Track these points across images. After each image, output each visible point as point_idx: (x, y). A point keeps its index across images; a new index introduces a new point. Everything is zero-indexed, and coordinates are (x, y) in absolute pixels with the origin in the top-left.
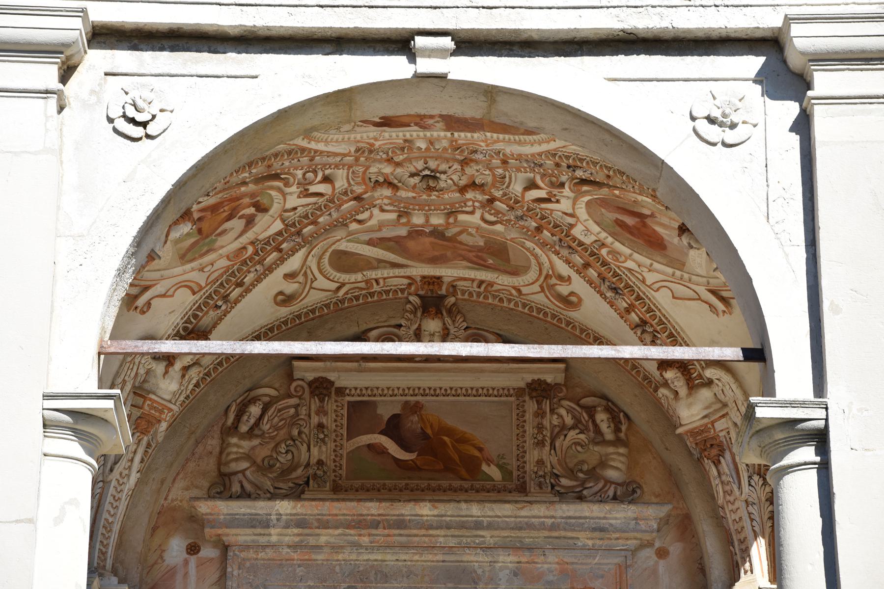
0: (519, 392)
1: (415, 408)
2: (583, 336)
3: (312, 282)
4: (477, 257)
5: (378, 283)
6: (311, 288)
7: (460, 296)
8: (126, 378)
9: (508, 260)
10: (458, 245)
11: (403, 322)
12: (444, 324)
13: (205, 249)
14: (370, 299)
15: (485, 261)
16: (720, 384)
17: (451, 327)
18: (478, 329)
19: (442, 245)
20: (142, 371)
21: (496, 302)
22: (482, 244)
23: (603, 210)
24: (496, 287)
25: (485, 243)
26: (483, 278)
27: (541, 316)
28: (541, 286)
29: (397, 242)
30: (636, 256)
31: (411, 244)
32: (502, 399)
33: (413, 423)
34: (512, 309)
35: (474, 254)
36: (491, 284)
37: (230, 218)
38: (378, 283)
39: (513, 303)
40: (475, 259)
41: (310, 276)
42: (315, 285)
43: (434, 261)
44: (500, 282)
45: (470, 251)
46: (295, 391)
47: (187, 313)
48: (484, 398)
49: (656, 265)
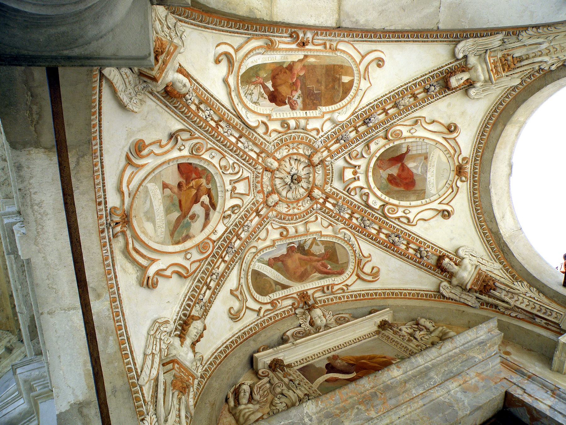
0: (377, 333)
1: (335, 357)
5: (279, 303)
8: (154, 351)
9: (337, 261)
10: (312, 257)
15: (326, 267)
19: (304, 260)
20: (164, 346)
22: (323, 251)
23: (381, 171)
24: (336, 288)
26: (328, 283)
27: (362, 298)
28: (358, 275)
29: (282, 261)
30: (402, 203)
32: (372, 338)
33: (339, 363)
34: (346, 301)
35: (320, 263)
36: (333, 285)
37: (196, 200)
38: (279, 303)
40: (321, 268)
43: (302, 277)
44: (337, 283)
45: (318, 261)
46: (262, 373)
48: (364, 341)
49: (413, 203)
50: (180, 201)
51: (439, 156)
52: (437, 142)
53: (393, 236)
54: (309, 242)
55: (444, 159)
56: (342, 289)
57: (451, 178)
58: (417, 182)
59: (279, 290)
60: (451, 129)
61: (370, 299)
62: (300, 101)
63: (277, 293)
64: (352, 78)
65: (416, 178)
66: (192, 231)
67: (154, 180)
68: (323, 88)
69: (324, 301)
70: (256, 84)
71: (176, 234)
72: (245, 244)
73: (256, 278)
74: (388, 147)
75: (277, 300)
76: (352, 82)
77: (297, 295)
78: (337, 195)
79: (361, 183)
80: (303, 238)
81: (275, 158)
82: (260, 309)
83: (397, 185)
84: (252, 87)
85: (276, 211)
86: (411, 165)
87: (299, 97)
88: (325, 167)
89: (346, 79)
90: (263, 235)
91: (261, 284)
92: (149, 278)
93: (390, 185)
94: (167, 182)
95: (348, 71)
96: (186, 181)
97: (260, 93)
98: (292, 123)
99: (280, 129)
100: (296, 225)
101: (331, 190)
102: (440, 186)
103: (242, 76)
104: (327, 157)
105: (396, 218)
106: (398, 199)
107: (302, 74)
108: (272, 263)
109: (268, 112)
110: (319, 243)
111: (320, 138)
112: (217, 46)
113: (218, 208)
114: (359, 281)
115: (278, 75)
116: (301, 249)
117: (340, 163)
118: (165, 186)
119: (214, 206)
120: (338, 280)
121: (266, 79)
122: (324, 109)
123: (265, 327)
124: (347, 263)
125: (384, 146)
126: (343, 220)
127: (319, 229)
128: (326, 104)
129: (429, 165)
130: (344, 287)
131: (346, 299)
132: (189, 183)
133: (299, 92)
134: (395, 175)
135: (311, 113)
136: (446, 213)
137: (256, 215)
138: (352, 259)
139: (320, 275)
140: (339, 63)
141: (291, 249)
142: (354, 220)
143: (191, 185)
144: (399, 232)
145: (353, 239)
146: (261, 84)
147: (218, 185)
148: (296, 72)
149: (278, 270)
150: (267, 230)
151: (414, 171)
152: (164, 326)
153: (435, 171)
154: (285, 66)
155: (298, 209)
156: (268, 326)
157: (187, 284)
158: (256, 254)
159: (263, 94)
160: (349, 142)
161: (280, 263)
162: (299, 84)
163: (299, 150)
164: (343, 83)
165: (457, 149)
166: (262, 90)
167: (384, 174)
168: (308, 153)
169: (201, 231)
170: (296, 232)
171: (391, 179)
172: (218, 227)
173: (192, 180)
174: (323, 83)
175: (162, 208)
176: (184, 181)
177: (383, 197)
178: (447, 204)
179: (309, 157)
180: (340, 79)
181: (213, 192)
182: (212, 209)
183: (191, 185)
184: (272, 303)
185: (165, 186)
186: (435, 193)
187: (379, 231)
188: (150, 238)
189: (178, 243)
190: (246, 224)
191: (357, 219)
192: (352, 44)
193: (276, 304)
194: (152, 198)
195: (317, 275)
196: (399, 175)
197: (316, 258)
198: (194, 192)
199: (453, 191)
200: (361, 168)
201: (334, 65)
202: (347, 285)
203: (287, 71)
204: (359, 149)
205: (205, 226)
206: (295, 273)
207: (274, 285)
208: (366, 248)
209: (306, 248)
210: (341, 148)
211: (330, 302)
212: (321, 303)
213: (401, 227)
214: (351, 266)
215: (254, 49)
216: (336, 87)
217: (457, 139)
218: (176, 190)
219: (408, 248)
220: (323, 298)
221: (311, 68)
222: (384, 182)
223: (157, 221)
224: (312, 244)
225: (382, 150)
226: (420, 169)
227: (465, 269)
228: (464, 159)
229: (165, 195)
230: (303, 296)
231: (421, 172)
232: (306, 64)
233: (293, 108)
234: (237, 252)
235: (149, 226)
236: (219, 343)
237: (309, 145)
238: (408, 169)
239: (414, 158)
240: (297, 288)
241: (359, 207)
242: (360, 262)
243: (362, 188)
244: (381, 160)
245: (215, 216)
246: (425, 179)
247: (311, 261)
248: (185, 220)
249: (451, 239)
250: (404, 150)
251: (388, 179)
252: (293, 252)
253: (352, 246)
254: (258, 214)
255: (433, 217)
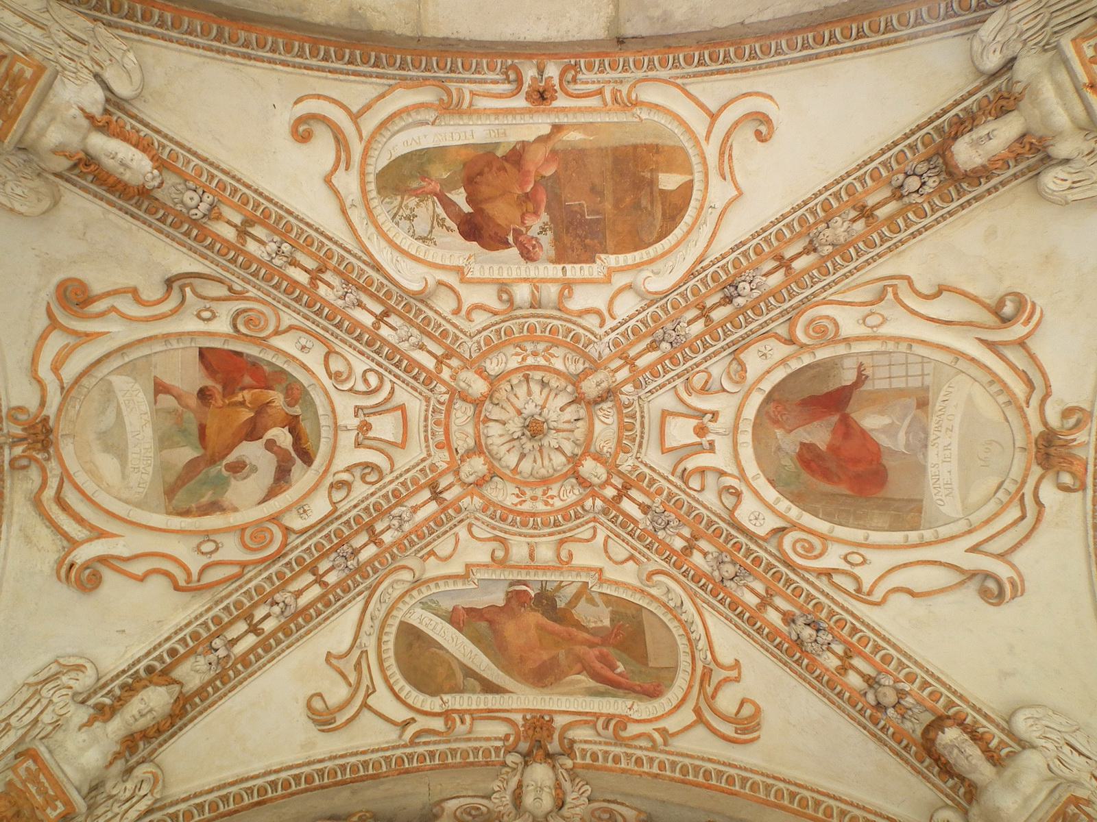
2: (772, 798)
3: (367, 695)
4: (603, 658)
5: (463, 722)
6: (365, 705)
7: (579, 761)
8: (13, 721)
9: (643, 659)
11: (496, 785)
12: (557, 780)
13: (205, 499)
14: (450, 761)
15: (613, 668)
16: (1050, 745)
17: (567, 785)
18: (609, 801)
19: (552, 633)
20: (47, 718)
21: (632, 766)
22: (607, 622)
23: (779, 433)
24: (633, 730)
25: (612, 620)
26: (612, 711)
27: (701, 779)
28: (697, 711)
29: (491, 622)
31: (510, 629)
34: (656, 776)
36: (623, 721)
37: (252, 432)
38: (463, 722)
39: (656, 764)
41: (366, 681)
42: (370, 701)
44: (636, 717)
45: (592, 645)
47: (160, 645)
49: (877, 537)
50: (202, 429)
51: (970, 399)
52: (959, 355)
53: (801, 621)
54: (570, 591)
55: (988, 407)
56: (650, 737)
57: (1016, 472)
58: (892, 476)
59: (474, 692)
60: (1008, 311)
61: (723, 791)
62: (546, 240)
63: (466, 696)
64: (686, 178)
65: (888, 462)
66: (230, 497)
67: (129, 369)
68: (608, 206)
69: (594, 756)
70: (421, 195)
71: (181, 495)
72: (388, 560)
73: (410, 646)
74: (795, 365)
75: (461, 713)
76: (688, 187)
77: (524, 718)
78: (652, 482)
79: (719, 459)
80: (554, 577)
81: (481, 372)
82: (406, 724)
83: (827, 475)
84: (413, 202)
85: (482, 497)
86: (871, 421)
87: (543, 230)
88: (620, 407)
89: (669, 181)
90: (444, 546)
91: (419, 660)
92: (72, 566)
93: (805, 476)
94: (167, 380)
95: (673, 158)
96: (224, 388)
97: (435, 216)
98: (522, 293)
99: (496, 305)
100: (537, 540)
101: (635, 468)
102: (975, 496)
103: (381, 176)
104: (625, 382)
105: (821, 573)
106: (828, 517)
107: (549, 172)
108: (463, 619)
109: (461, 262)
110: (598, 599)
111: (607, 333)
112: (296, 103)
113: (317, 462)
114: (700, 731)
115: (481, 174)
116: (545, 601)
117: (665, 400)
118: (160, 388)
119: (307, 458)
120: (643, 709)
121: (450, 184)
122: (612, 260)
123: (407, 772)
124: (673, 670)
125: (784, 362)
126: (664, 549)
127: (603, 565)
128: (620, 249)
129: (933, 425)
130: (656, 736)
131: (655, 770)
132: (233, 393)
133: (545, 217)
134: (823, 447)
135: (574, 271)
136: (991, 585)
137: (431, 499)
138: (684, 661)
139: (592, 683)
140: (650, 140)
141: (516, 598)
142: (697, 558)
143: (239, 398)
144: (823, 615)
145: (688, 605)
146: (436, 195)
147: (321, 411)
148: (532, 168)
149: (477, 640)
150: (456, 535)
151: (883, 440)
152: (73, 674)
153: (955, 448)
154: (500, 153)
155: (547, 503)
156: (418, 770)
157: (195, 607)
158: (417, 583)
159: (443, 220)
160: (681, 348)
161: (484, 624)
162: (543, 198)
163: (553, 360)
164: (662, 192)
165: (1037, 382)
166: (440, 210)
167: (789, 441)
168: (577, 367)
169: (259, 503)
170: (532, 557)
171: (809, 458)
172: (311, 502)
173: (243, 389)
174: (608, 194)
175: (149, 431)
176: (219, 387)
177: (784, 505)
178: (1001, 556)
179: (576, 380)
180: (652, 183)
181: (306, 426)
182: (299, 461)
183: (239, 398)
184: (446, 715)
185: (160, 388)
186: (954, 515)
187: (765, 602)
188: (108, 490)
189: (186, 513)
190: (395, 512)
191: (705, 554)
192: (677, 86)
193: (454, 721)
194: (123, 407)
195: (585, 680)
196: (833, 449)
197: (586, 635)
198: (246, 414)
199: (1023, 517)
200: (720, 419)
201: (635, 147)
202: (663, 732)
203: (507, 166)
204: (717, 368)
205: (271, 494)
206: (522, 660)
207: (459, 675)
208: (728, 641)
209: (561, 604)
210: (661, 361)
211: (610, 764)
212: (583, 758)
213: (833, 599)
214: (681, 681)
215: (406, 110)
216: (645, 202)
217: (1032, 344)
218: (193, 402)
219: (844, 669)
220: (596, 748)
221: (575, 158)
222: (790, 464)
223: (131, 456)
224: (577, 597)
225: (780, 375)
226: (902, 436)
227: (1012, 785)
228: (1067, 413)
229: (159, 406)
230: (539, 725)
231: (907, 445)
232: (559, 146)
233: (528, 255)
234: (359, 569)
235: (108, 465)
236: (257, 767)
237: (576, 346)
238: (863, 432)
239: (882, 400)
240: (525, 699)
241: (711, 523)
242: (707, 675)
243: (722, 473)
244: (779, 402)
245: (303, 478)
246: (923, 469)
247: (571, 639)
248: (213, 471)
249: (1005, 675)
250: (849, 377)
251: (800, 457)
252: (522, 605)
253: (686, 626)
254: (436, 495)
255: (942, 591)
